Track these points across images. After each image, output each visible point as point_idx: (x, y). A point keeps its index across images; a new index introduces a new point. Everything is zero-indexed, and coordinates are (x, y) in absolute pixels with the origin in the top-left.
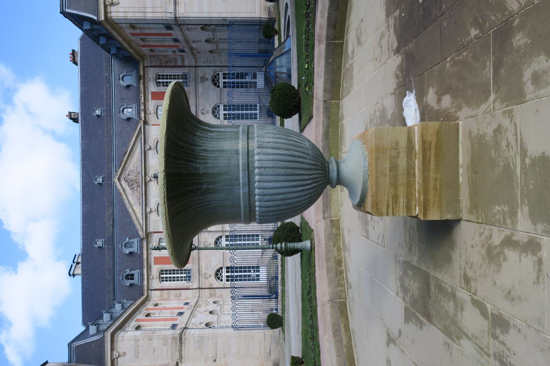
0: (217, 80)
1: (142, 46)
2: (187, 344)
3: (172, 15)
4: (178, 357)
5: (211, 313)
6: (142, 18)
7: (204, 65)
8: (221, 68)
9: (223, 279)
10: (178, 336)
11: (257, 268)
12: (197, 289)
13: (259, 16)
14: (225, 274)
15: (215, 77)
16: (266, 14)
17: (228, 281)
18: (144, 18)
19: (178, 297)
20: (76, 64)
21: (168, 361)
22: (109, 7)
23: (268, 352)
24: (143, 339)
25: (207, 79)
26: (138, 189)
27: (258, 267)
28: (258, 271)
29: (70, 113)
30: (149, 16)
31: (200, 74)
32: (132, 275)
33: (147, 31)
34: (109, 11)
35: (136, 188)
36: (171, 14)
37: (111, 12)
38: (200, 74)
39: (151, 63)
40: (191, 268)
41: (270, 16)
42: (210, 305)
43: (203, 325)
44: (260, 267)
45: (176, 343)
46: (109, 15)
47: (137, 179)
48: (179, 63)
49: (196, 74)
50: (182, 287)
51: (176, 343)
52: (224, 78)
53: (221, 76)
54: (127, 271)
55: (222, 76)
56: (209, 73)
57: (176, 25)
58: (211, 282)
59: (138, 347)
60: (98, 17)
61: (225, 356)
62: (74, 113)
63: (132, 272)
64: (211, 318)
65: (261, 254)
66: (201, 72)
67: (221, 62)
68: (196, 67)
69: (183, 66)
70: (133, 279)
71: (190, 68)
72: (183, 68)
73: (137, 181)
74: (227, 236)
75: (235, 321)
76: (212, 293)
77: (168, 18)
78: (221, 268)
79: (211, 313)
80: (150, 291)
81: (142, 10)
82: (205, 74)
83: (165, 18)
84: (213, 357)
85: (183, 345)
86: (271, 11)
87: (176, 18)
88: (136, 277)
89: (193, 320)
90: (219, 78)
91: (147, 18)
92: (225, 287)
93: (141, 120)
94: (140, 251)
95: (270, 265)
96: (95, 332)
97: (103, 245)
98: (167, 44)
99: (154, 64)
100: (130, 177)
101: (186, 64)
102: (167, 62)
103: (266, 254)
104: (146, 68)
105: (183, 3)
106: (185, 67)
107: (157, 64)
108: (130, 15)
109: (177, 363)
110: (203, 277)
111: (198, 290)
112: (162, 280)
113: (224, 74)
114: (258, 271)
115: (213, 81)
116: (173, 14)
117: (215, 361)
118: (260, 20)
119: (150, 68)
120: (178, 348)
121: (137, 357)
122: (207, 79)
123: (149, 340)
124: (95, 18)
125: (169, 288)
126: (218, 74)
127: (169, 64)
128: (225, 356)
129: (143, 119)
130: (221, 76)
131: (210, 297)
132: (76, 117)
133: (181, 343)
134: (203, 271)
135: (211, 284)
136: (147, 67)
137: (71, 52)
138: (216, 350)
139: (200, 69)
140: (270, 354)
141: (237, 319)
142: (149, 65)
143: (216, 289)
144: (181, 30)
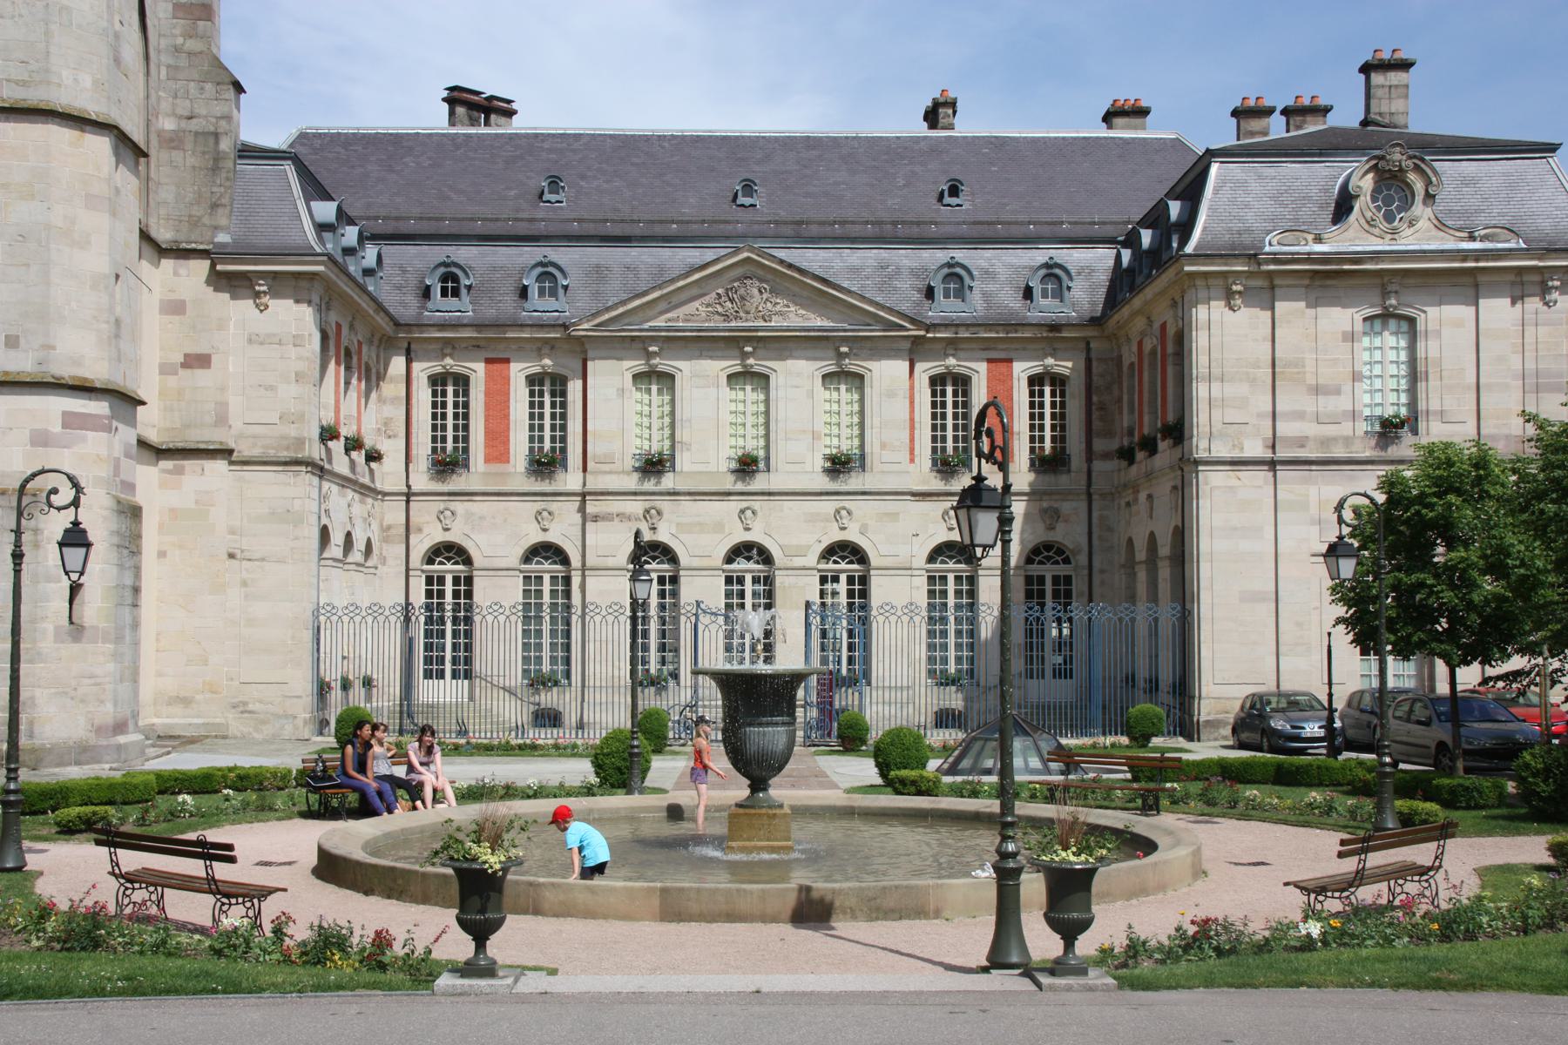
0: (1048, 558)
1: (1140, 344)
2: (282, 477)
3: (1201, 454)
4: (246, 453)
5: (349, 535)
6: (1194, 371)
7: (1095, 520)
8: (1086, 572)
9: (436, 567)
10: (307, 454)
11: (465, 671)
12: (409, 486)
13: (1203, 695)
14: (449, 569)
15: (1060, 552)
16: (1209, 714)
17: (429, 581)
18: (1194, 376)
19: (385, 429)
20: (1108, 118)
21: (236, 423)
22: (1220, 282)
23: (251, 707)
24: (300, 358)
25: (1051, 528)
26: (717, 317)
27: (468, 675)
28: (455, 675)
29: (953, 104)
30: (1200, 392)
31: (1066, 507)
32: (456, 293)
33: (1170, 370)
34: (1211, 281)
35: (720, 309)
36: (1205, 450)
37: (1208, 287)
38: (1066, 507)
39: (1098, 359)
40: (472, 469)
41: (1205, 727)
42: (365, 530)
43: (325, 521)
44: (466, 682)
45: (288, 448)
46: (1199, 282)
47: (748, 313)
48: (1099, 445)
49: (1065, 494)
50: (414, 440)
51: (288, 448)
52: (1056, 580)
53: (1062, 570)
54: (468, 278)
55: (1062, 574)
56: (1071, 534)
57: (1181, 459)
58: (426, 531)
59: (280, 344)
60: (1189, 255)
61: (244, 584)
62: (955, 113)
63: (464, 291)
64: (337, 538)
65: (507, 684)
66: (1074, 508)
67: (1102, 571)
68: (1089, 495)
69: (1090, 455)
70: (444, 293)
71: (1085, 477)
72: (1084, 455)
73: (742, 314)
74: (567, 580)
75: (340, 613)
76: (393, 532)
77: (1195, 440)
78: (468, 561)
79: (349, 535)
80: (406, 345)
81: (1216, 371)
82: (1066, 521)
83: (1195, 432)
84: (242, 551)
85: (280, 468)
86: (1218, 728)
87: (1197, 462)
88: (452, 302)
89: (335, 488)
90: (1057, 563)
91: (1194, 385)
92: (411, 573)
93: (927, 332)
94: (530, 317)
95: (483, 714)
96: (320, 218)
97: (549, 202)
98: (1146, 419)
99: (1095, 370)
100: (755, 291)
101: (1098, 465)
102: (1102, 408)
103: (495, 695)
104: (1082, 345)
105: (1237, 483)
106: (1089, 460)
107: (1095, 378)
108: (1200, 342)
109: (231, 452)
110: (442, 506)
111: (405, 489)
112: (437, 381)
113: (1068, 579)
114: (455, 675)
115: (1048, 546)
116: (1206, 455)
117: (232, 556)
118: (1194, 697)
119: (1083, 356)
120: (272, 452)
121: (250, 341)
122: (1051, 528)
123: (297, 374)
124: (1189, 249)
125: (414, 401)
126: (1067, 561)
127: (1095, 415)
128: (244, 584)
129: (929, 335)
130: (1062, 570)
131: (382, 525)
132: (942, 121)
133: (286, 463)
134: (460, 506)
135: (420, 530)
136: (1088, 350)
137: (1144, 104)
138: (263, 560)
139: (1083, 506)
140: (242, 712)
141: (346, 619)
142: (1093, 355)
143: (404, 546)
144: (1171, 468)
